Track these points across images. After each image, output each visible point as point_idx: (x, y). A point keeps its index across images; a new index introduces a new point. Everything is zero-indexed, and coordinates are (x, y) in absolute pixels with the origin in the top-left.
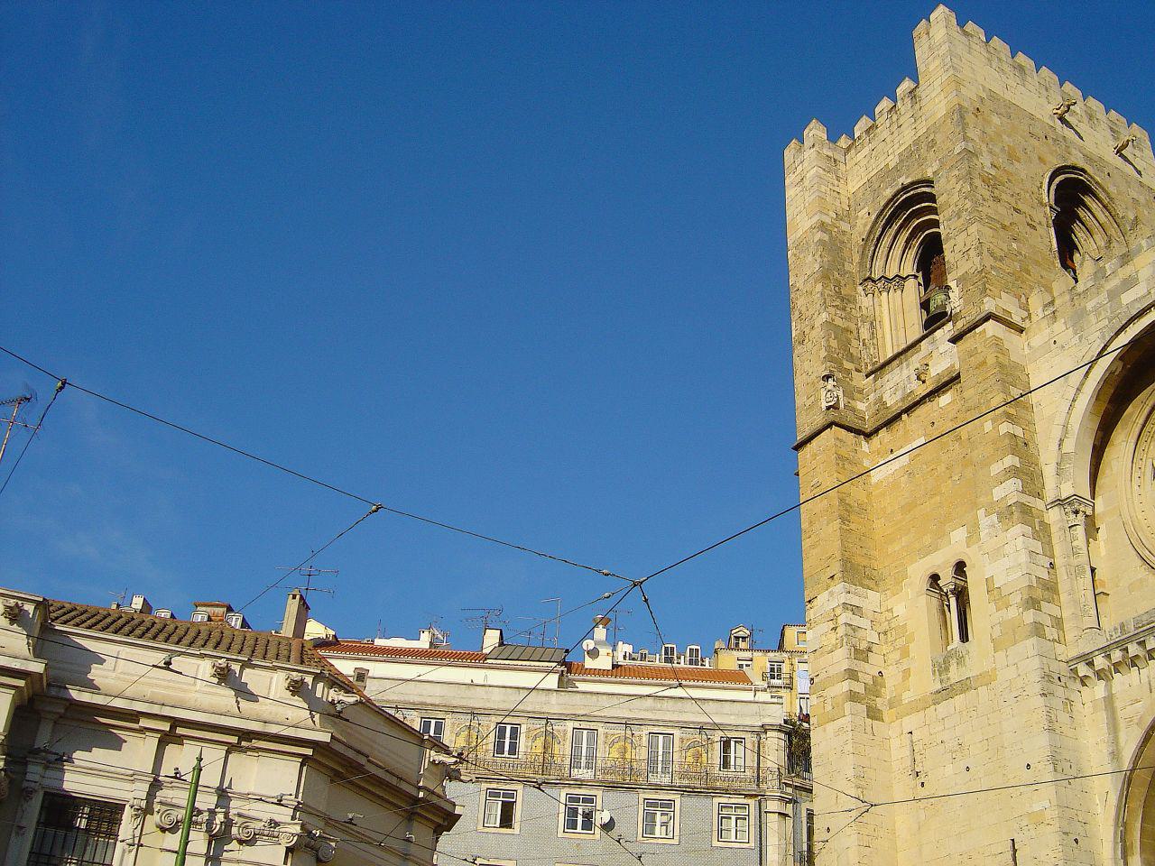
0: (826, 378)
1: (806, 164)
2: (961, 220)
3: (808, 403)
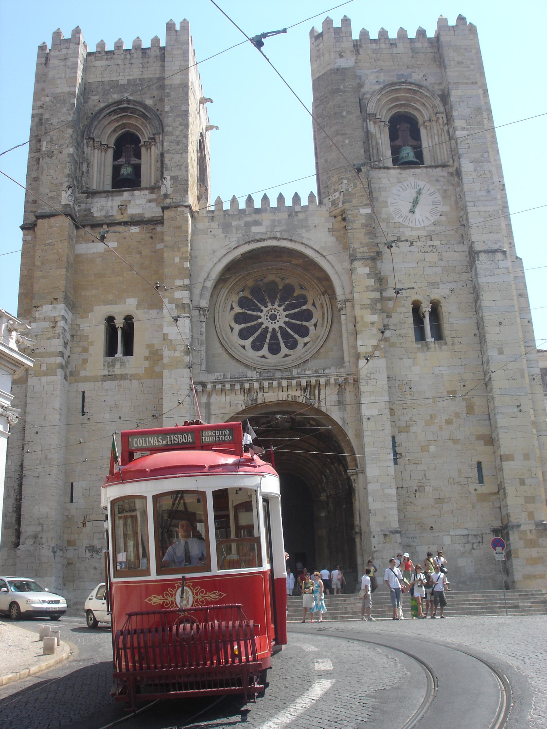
0: (70, 187)
1: (70, 51)
2: (179, 147)
3: (51, 194)
